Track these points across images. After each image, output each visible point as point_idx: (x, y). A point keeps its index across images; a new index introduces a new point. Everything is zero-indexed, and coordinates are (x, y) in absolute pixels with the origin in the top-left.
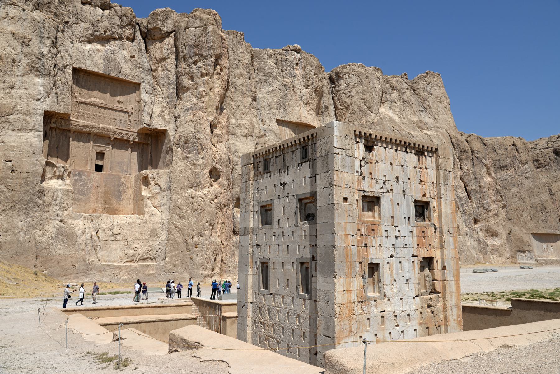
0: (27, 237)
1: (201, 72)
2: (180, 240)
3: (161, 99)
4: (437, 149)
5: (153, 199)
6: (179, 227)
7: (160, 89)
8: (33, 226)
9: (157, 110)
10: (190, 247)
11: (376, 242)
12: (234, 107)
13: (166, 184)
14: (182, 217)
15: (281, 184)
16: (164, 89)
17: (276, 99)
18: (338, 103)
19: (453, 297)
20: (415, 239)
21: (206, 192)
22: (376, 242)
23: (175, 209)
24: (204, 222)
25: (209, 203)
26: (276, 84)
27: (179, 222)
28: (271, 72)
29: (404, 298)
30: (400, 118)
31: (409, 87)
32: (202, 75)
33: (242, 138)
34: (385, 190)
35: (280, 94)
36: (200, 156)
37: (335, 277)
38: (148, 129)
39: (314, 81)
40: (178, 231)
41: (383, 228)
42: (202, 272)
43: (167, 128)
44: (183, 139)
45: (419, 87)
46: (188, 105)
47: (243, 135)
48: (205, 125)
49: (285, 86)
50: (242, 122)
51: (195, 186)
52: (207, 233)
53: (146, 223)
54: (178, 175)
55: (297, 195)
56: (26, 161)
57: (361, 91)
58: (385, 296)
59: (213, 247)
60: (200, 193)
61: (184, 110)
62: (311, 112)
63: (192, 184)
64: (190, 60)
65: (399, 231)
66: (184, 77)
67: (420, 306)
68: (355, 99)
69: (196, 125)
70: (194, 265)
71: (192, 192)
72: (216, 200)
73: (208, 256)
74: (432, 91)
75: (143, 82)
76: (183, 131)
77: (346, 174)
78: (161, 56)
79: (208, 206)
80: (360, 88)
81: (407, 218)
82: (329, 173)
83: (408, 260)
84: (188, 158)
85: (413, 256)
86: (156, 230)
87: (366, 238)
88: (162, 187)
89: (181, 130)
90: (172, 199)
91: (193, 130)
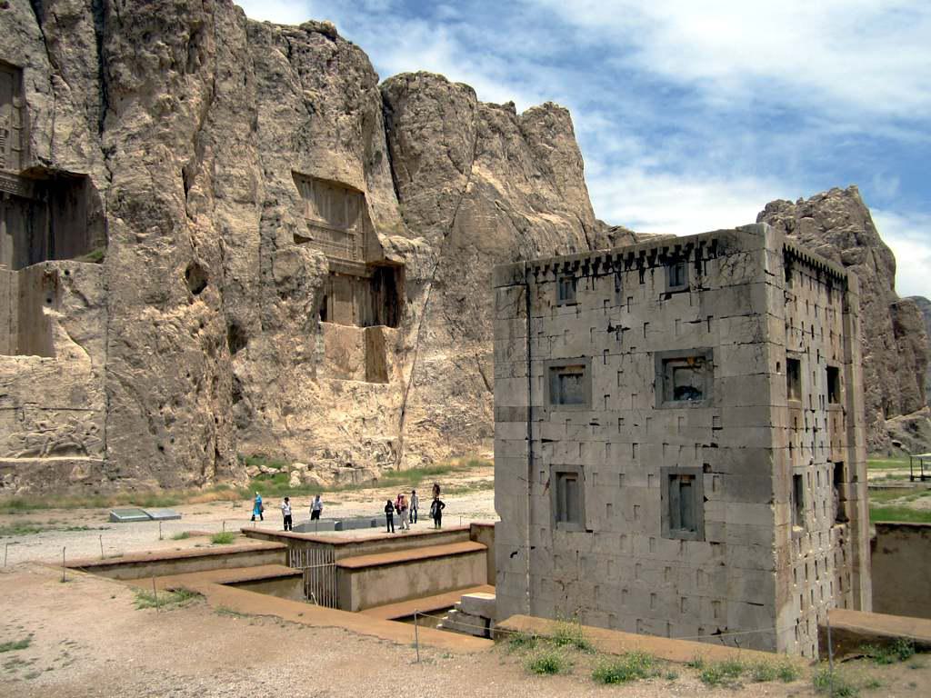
1: (161, 59)
2: (136, 411)
3: (70, 107)
5: (70, 324)
6: (132, 383)
7: (65, 85)
9: (63, 128)
10: (158, 425)
12: (217, 139)
13: (97, 294)
14: (137, 364)
15: (610, 329)
16: (76, 86)
17: (290, 130)
18: (396, 147)
21: (182, 314)
23: (121, 347)
24: (182, 374)
25: (189, 336)
26: (290, 100)
27: (130, 373)
28: (281, 72)
30: (506, 187)
31: (517, 129)
32: (163, 66)
33: (234, 204)
35: (299, 120)
36: (165, 238)
37: (771, 502)
38: (45, 171)
39: (361, 101)
40: (130, 394)
42: (182, 475)
43: (89, 172)
44: (128, 200)
45: (534, 131)
46: (134, 126)
47: (237, 198)
48: (173, 172)
49: (307, 104)
50: (234, 172)
51: (161, 300)
52: (189, 396)
53: (59, 373)
54: (121, 275)
55: (656, 353)
57: (441, 128)
59: (201, 426)
60: (171, 315)
61: (124, 137)
62: (356, 163)
63: (152, 297)
64: (136, 30)
66: (122, 65)
68: (431, 143)
69: (154, 172)
70: (167, 461)
71: (154, 313)
72: (201, 332)
73: (193, 443)
74: (555, 141)
75: (30, 65)
76: (127, 183)
78: (66, 12)
79: (189, 342)
80: (439, 123)
82: (753, 319)
84: (139, 240)
86: (81, 388)
88: (88, 298)
89: (122, 181)
90: (111, 325)
91: (148, 181)
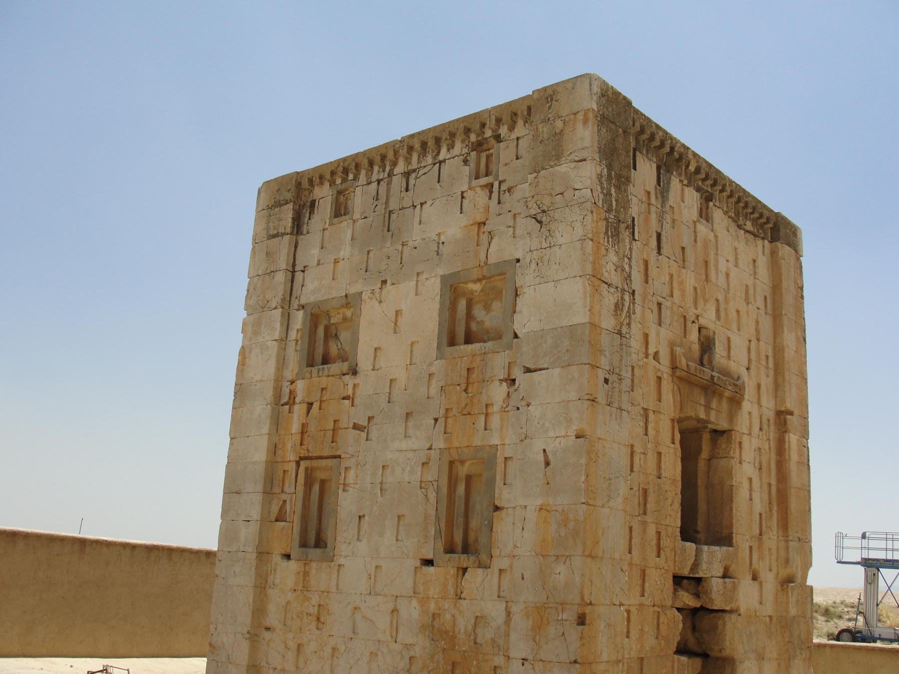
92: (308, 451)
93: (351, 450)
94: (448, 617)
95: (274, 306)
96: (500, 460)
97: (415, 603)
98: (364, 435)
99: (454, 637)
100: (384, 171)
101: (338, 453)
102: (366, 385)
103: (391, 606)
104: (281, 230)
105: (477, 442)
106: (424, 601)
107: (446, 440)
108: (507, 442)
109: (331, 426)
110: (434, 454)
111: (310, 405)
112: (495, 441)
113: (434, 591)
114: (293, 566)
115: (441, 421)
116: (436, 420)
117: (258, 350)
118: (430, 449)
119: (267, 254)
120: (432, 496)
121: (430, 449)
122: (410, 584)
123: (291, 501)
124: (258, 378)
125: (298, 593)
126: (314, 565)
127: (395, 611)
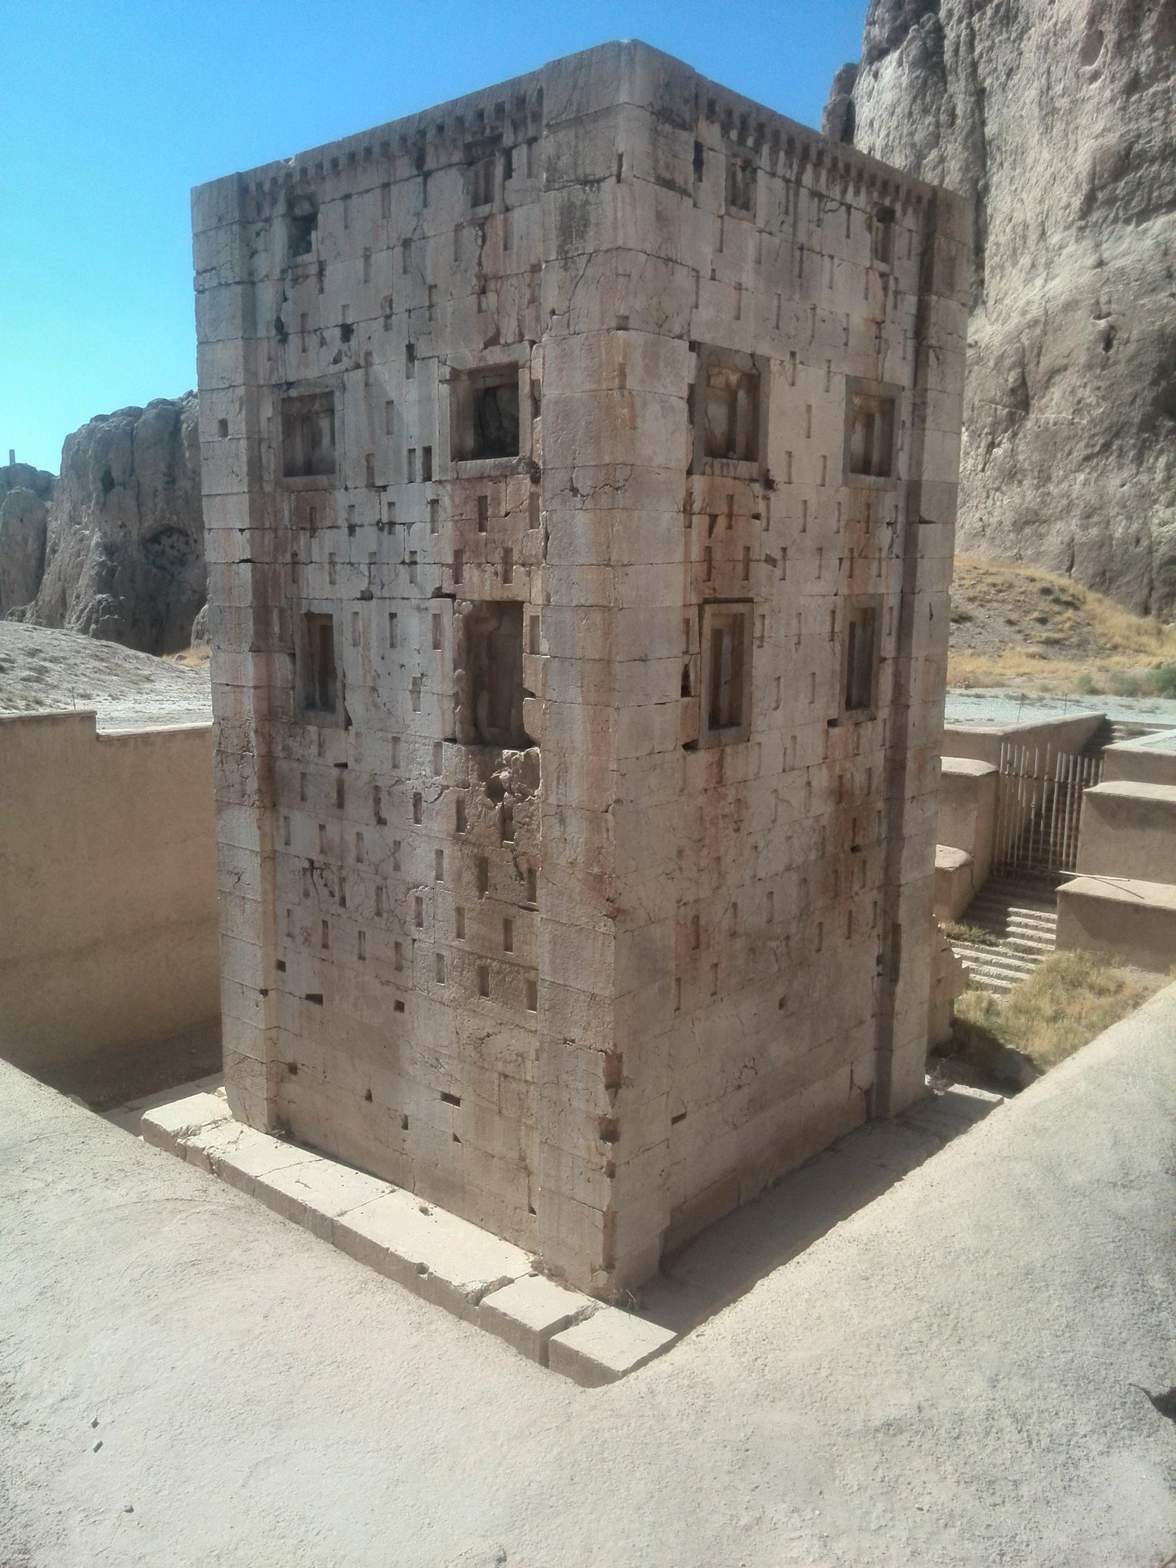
0: (1135, 526)
4: (541, 91)
8: (1150, 494)
11: (321, 548)
19: (574, 772)
20: (447, 529)
22: (321, 548)
29: (403, 737)
34: (346, 362)
41: (341, 499)
56: (1143, 305)
58: (349, 722)
65: (391, 505)
67: (461, 777)
77: (220, 346)
81: (419, 453)
83: (419, 609)
85: (439, 594)
87: (295, 538)
92: (714, 589)
93: (764, 591)
94: (849, 776)
95: (677, 330)
96: (886, 612)
97: (824, 769)
98: (778, 572)
99: (852, 795)
100: (791, 167)
101: (750, 596)
102: (780, 502)
103: (805, 778)
104: (680, 181)
105: (871, 590)
106: (830, 768)
107: (850, 586)
108: (891, 591)
109: (740, 555)
110: (839, 600)
111: (713, 518)
112: (883, 590)
113: (838, 754)
114: (703, 758)
115: (846, 564)
116: (841, 559)
117: (657, 407)
118: (836, 595)
119: (659, 216)
120: (838, 648)
121: (836, 595)
122: (820, 750)
123: (696, 665)
124: (659, 460)
125: (710, 793)
126: (728, 750)
127: (809, 784)
